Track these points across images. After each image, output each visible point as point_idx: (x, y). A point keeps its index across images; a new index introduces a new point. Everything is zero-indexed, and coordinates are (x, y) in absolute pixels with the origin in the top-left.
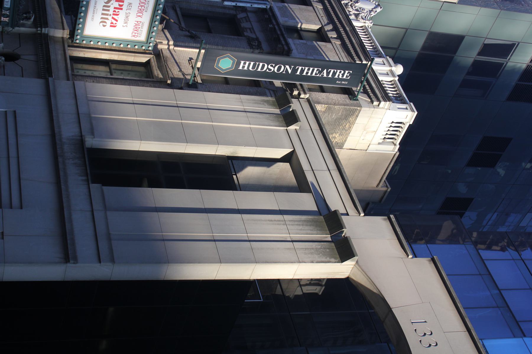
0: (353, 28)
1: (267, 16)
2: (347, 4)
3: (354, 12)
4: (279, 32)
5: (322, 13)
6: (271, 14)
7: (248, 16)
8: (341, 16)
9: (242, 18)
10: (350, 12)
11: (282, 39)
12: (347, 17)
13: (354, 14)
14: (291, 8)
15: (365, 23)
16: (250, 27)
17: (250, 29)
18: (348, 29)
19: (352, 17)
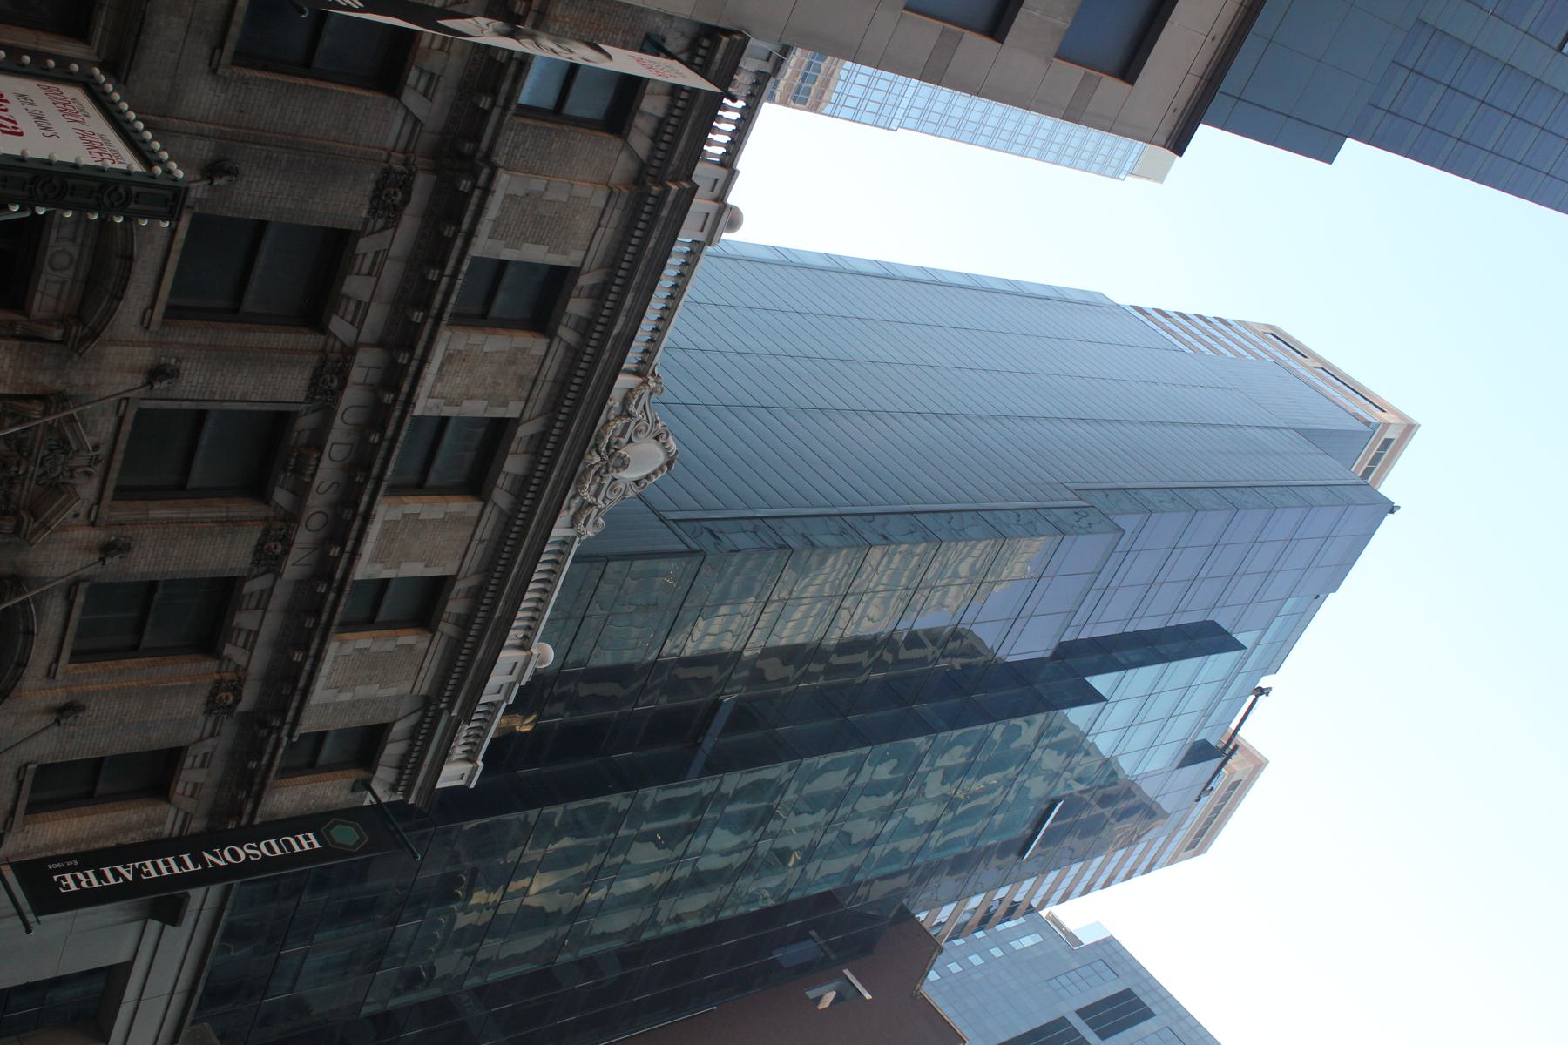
2: (592, 466)
4: (302, 683)
6: (324, 618)
8: (515, 570)
9: (251, 594)
11: (294, 704)
17: (250, 631)
18: (497, 614)
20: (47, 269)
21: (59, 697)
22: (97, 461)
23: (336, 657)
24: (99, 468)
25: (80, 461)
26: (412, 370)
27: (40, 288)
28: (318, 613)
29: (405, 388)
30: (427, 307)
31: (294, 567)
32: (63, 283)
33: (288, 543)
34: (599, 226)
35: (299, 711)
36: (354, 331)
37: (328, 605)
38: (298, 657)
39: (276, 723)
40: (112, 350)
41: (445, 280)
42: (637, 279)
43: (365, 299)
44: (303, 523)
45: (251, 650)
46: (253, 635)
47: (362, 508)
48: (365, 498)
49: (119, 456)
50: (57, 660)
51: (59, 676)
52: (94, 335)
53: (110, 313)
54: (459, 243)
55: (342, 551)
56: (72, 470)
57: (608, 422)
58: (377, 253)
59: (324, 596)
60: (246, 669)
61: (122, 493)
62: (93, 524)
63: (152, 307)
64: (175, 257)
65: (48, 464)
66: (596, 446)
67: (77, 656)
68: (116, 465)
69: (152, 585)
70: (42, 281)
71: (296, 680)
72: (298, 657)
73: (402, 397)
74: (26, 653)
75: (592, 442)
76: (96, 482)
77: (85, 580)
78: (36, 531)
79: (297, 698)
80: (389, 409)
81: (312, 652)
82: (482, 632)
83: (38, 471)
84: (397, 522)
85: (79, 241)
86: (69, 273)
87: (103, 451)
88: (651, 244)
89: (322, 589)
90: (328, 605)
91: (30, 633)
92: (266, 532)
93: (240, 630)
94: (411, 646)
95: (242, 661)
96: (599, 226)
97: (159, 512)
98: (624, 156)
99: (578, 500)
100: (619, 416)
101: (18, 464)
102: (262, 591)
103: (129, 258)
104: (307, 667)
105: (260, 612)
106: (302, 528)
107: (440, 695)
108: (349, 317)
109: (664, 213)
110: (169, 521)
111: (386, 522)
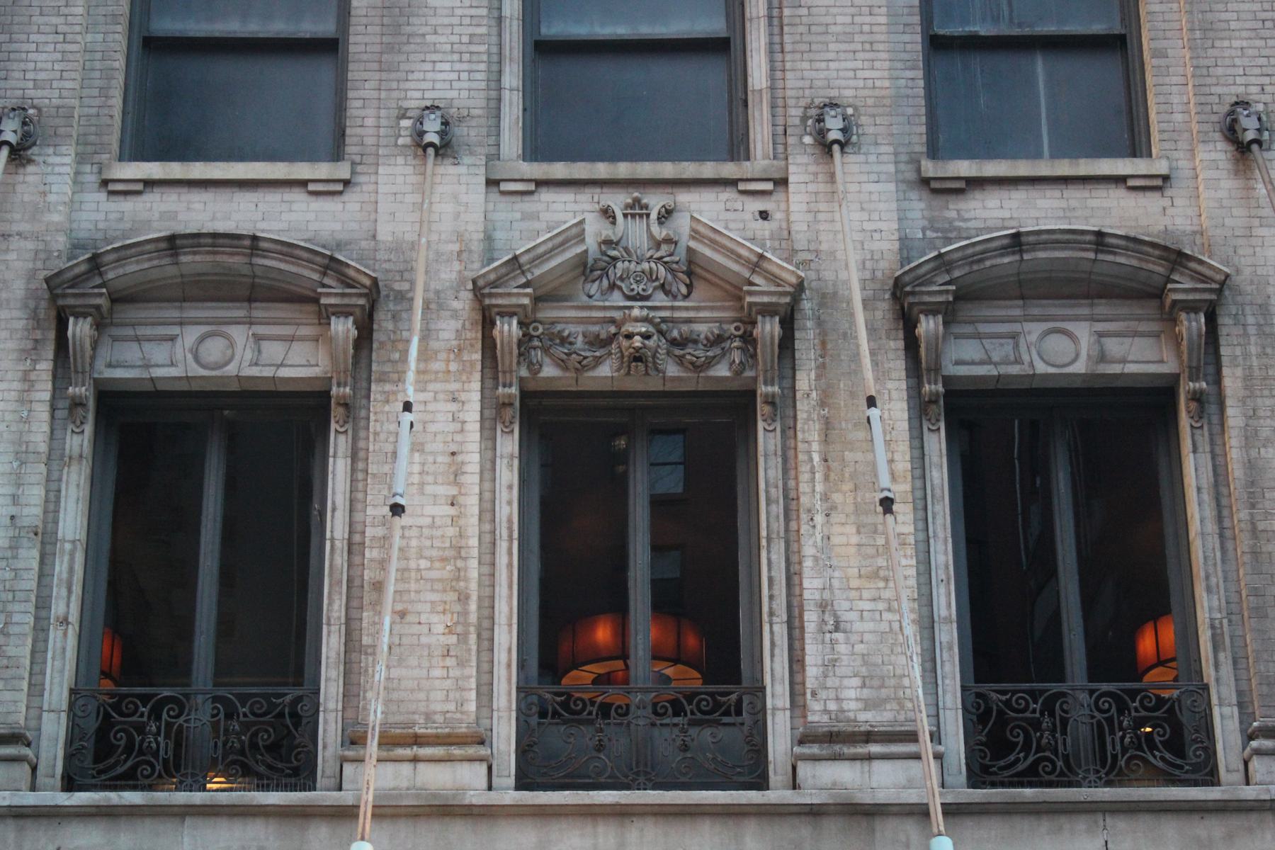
20: (231, 370)
21: (1218, 153)
22: (637, 201)
24: (656, 201)
25: (636, 234)
27: (268, 372)
32: (258, 339)
40: (384, 233)
49: (623, 170)
50: (1120, 180)
51: (1161, 167)
52: (332, 265)
53: (287, 250)
56: (658, 245)
61: (738, 147)
62: (782, 182)
63: (303, 183)
64: (198, 170)
65: (638, 289)
67: (1137, 145)
68: (646, 169)
69: (937, 45)
70: (255, 372)
74: (1070, 238)
76: (684, 197)
77: (919, 170)
78: (774, 279)
83: (660, 299)
85: (175, 330)
86: (239, 334)
87: (617, 200)
91: (1017, 242)
97: (758, 74)
101: (629, 336)
103: (173, 244)
110: (775, 49)
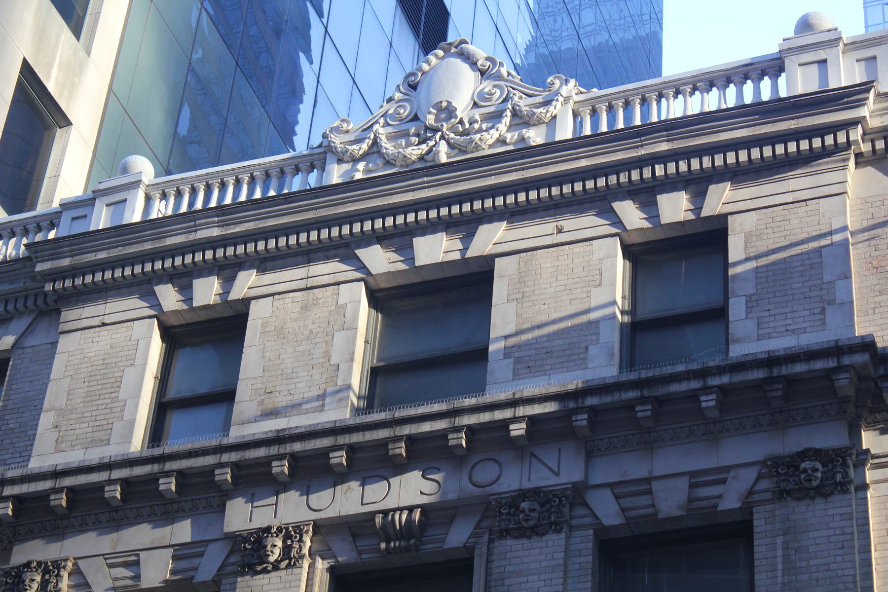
0: (578, 143)
1: (643, 411)
3: (503, 127)
5: (537, 231)
6: (632, 394)
7: (610, 486)
8: (583, 163)
9: (623, 510)
10: (502, 141)
11: (799, 368)
12: (524, 153)
13: (510, 128)
14: (517, 334)
15: (567, 99)
16: (684, 483)
17: (692, 486)
18: (664, 147)
19: (536, 136)
23: (759, 338)
26: (234, 457)
28: (630, 406)
29: (261, 452)
30: (152, 480)
31: (561, 469)
33: (523, 494)
34: (104, 324)
35: (810, 355)
36: (211, 546)
37: (607, 399)
38: (708, 401)
39: (843, 381)
41: (117, 474)
42: (148, 246)
43: (170, 551)
44: (488, 490)
45: (727, 469)
46: (696, 479)
47: (441, 425)
48: (427, 427)
54: (69, 482)
55: (515, 420)
57: (388, 163)
58: (111, 566)
59: (593, 411)
60: (763, 463)
66: (422, 158)
71: (759, 385)
72: (708, 401)
73: (274, 450)
75: (419, 165)
79: (785, 370)
80: (294, 458)
81: (695, 384)
82: (700, 152)
84: (518, 361)
88: (102, 255)
89: (581, 420)
90: (607, 399)
92: (505, 533)
93: (690, 500)
94: (748, 236)
95: (750, 474)
96: (104, 324)
98: (30, 342)
99: (509, 137)
100: (379, 152)
102: (617, 497)
104: (725, 379)
105: (655, 485)
106: (495, 488)
107: (837, 149)
108: (196, 561)
109: (66, 262)
111: (516, 376)
